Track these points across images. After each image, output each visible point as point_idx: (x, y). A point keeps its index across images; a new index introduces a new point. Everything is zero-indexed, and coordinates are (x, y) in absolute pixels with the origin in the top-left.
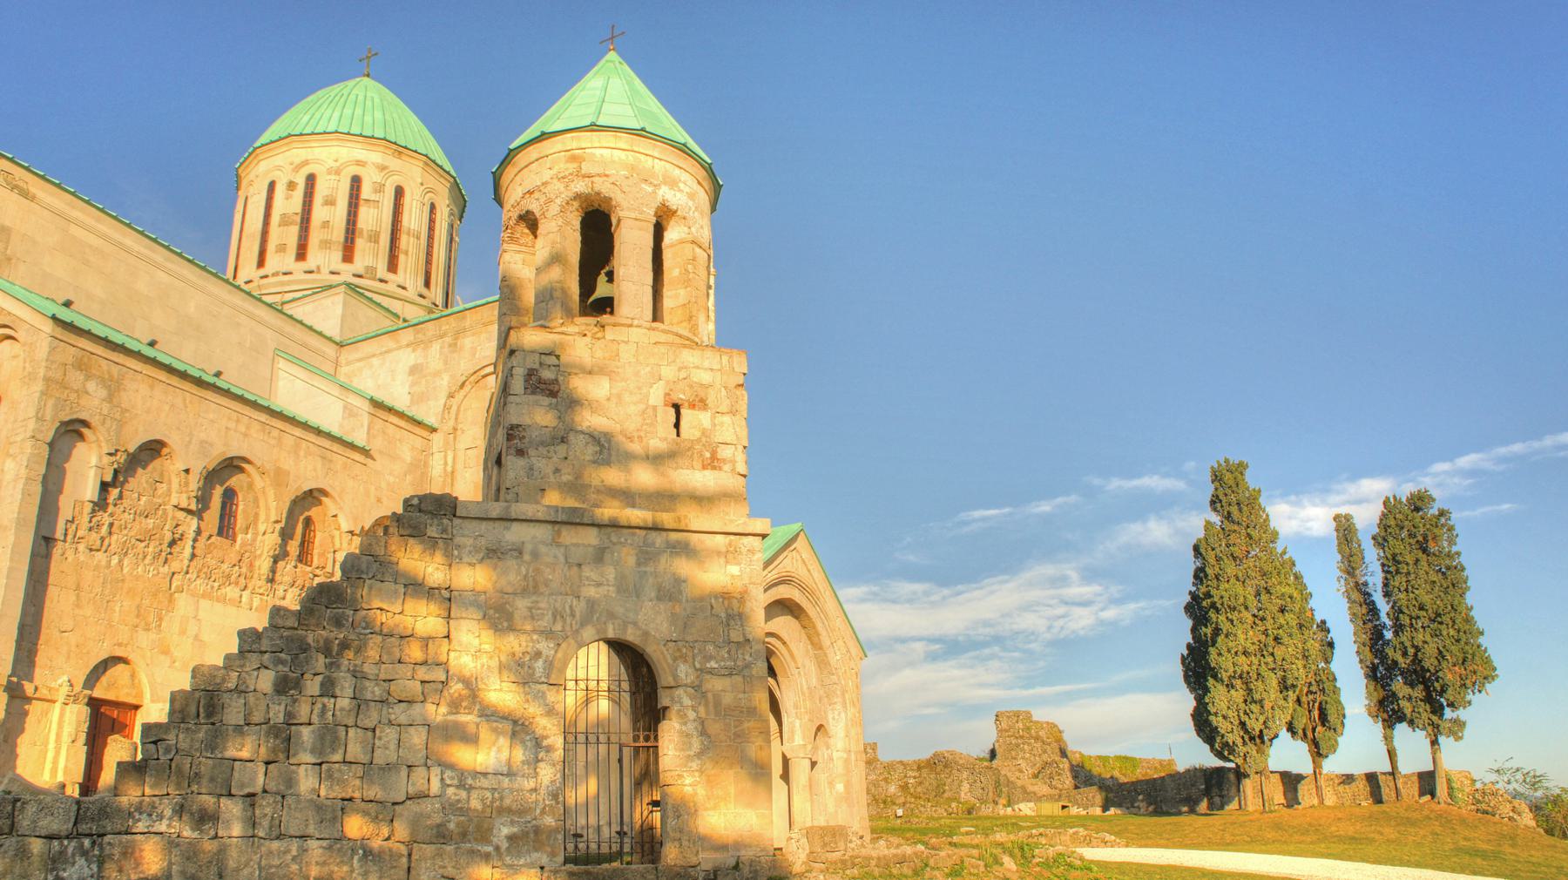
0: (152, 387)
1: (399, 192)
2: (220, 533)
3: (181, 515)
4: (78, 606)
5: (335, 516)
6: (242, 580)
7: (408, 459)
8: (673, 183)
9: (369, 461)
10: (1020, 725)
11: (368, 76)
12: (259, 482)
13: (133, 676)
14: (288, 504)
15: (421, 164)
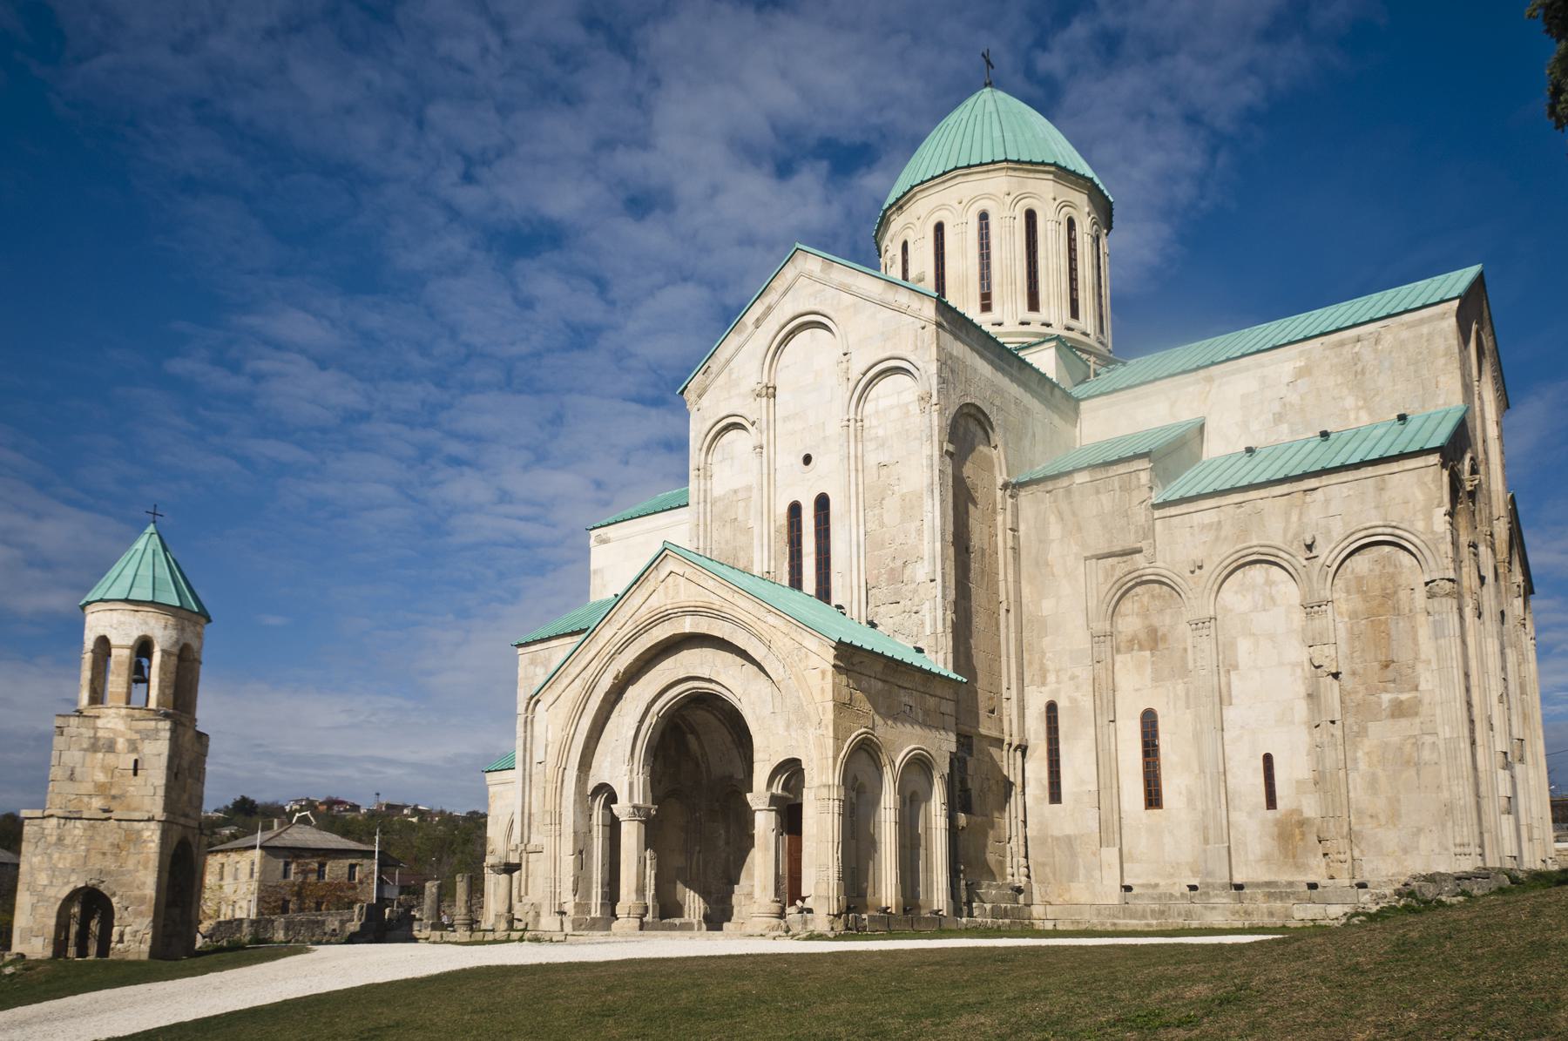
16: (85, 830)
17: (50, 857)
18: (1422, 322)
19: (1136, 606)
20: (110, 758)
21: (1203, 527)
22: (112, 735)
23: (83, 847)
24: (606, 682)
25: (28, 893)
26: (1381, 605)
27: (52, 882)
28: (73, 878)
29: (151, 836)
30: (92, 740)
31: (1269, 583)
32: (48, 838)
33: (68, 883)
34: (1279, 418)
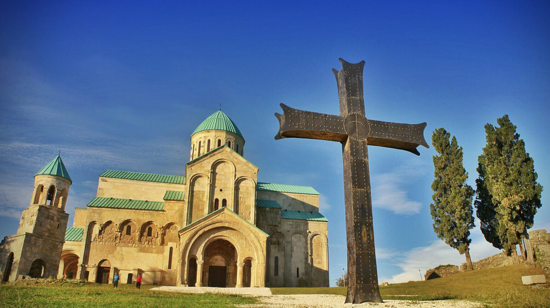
0: (108, 212)
1: (209, 141)
2: (127, 234)
3: (117, 233)
4: (97, 251)
5: (157, 225)
6: (133, 242)
7: (177, 209)
8: (41, 180)
9: (164, 212)
10: (540, 236)
11: (220, 110)
12: (135, 223)
13: (109, 262)
14: (141, 226)
15: (214, 132)
16: (42, 242)
17: (32, 248)
18: (315, 197)
19: (275, 236)
20: (52, 222)
21: (290, 225)
22: (53, 215)
23: (41, 247)
24: (200, 232)
25: (24, 258)
26: (317, 245)
27: (31, 256)
28: (37, 256)
29: (60, 247)
30: (48, 215)
31: (300, 237)
32: (32, 242)
33: (35, 257)
34: (289, 206)
